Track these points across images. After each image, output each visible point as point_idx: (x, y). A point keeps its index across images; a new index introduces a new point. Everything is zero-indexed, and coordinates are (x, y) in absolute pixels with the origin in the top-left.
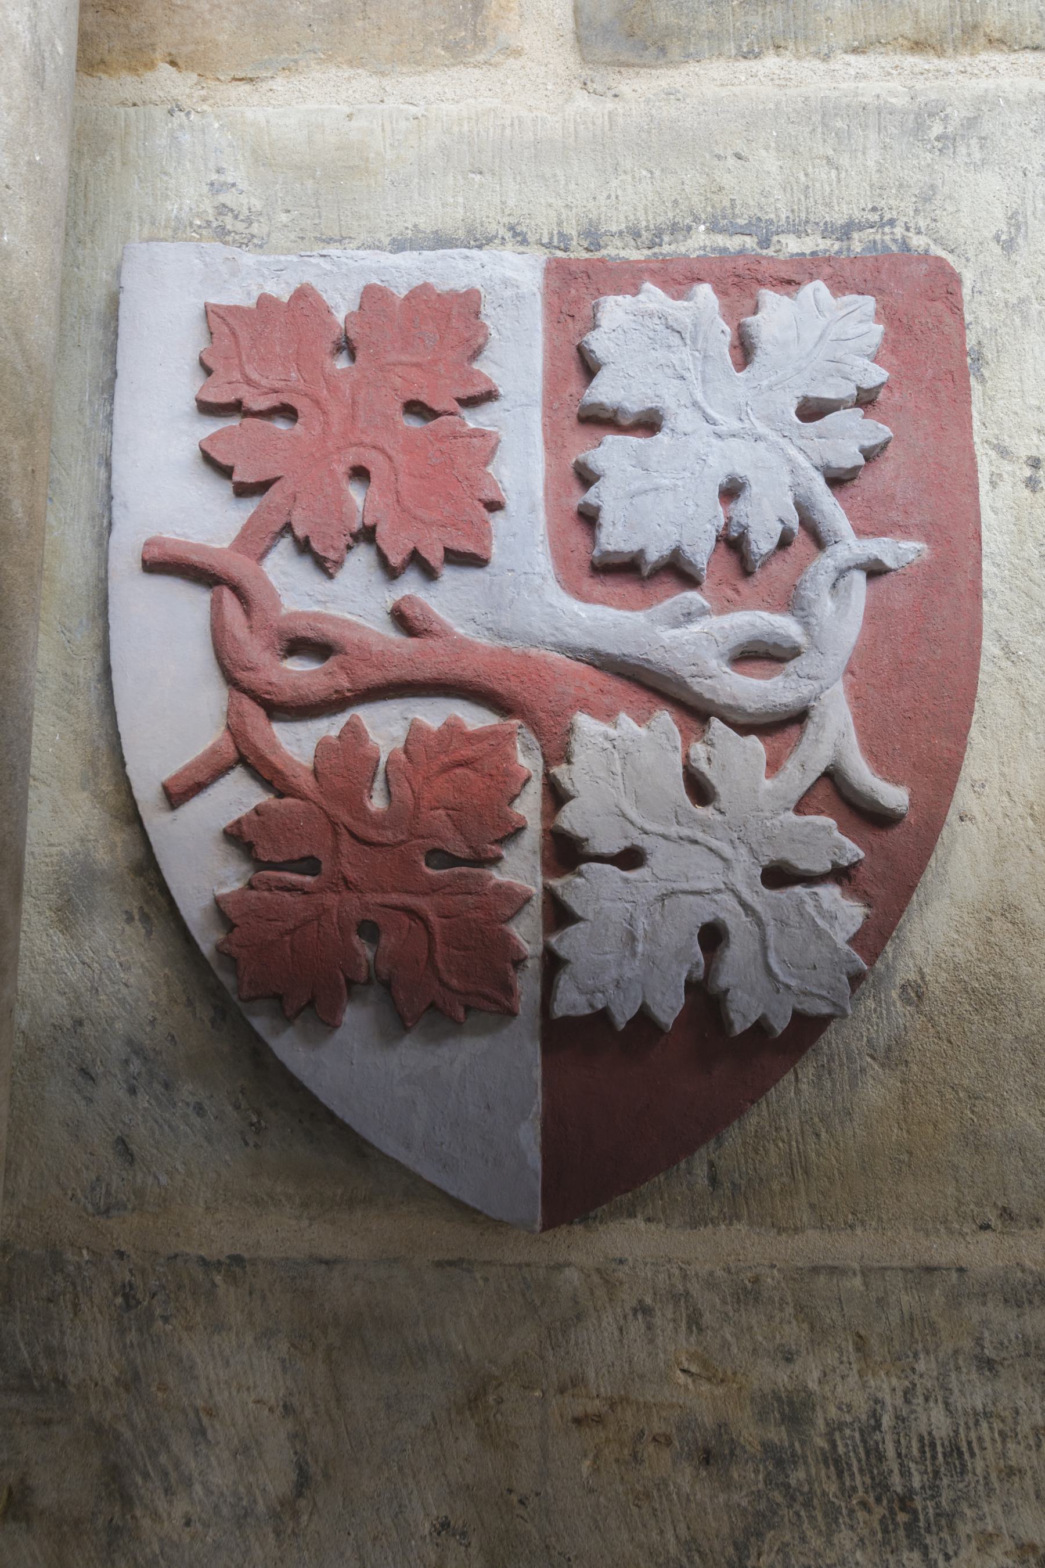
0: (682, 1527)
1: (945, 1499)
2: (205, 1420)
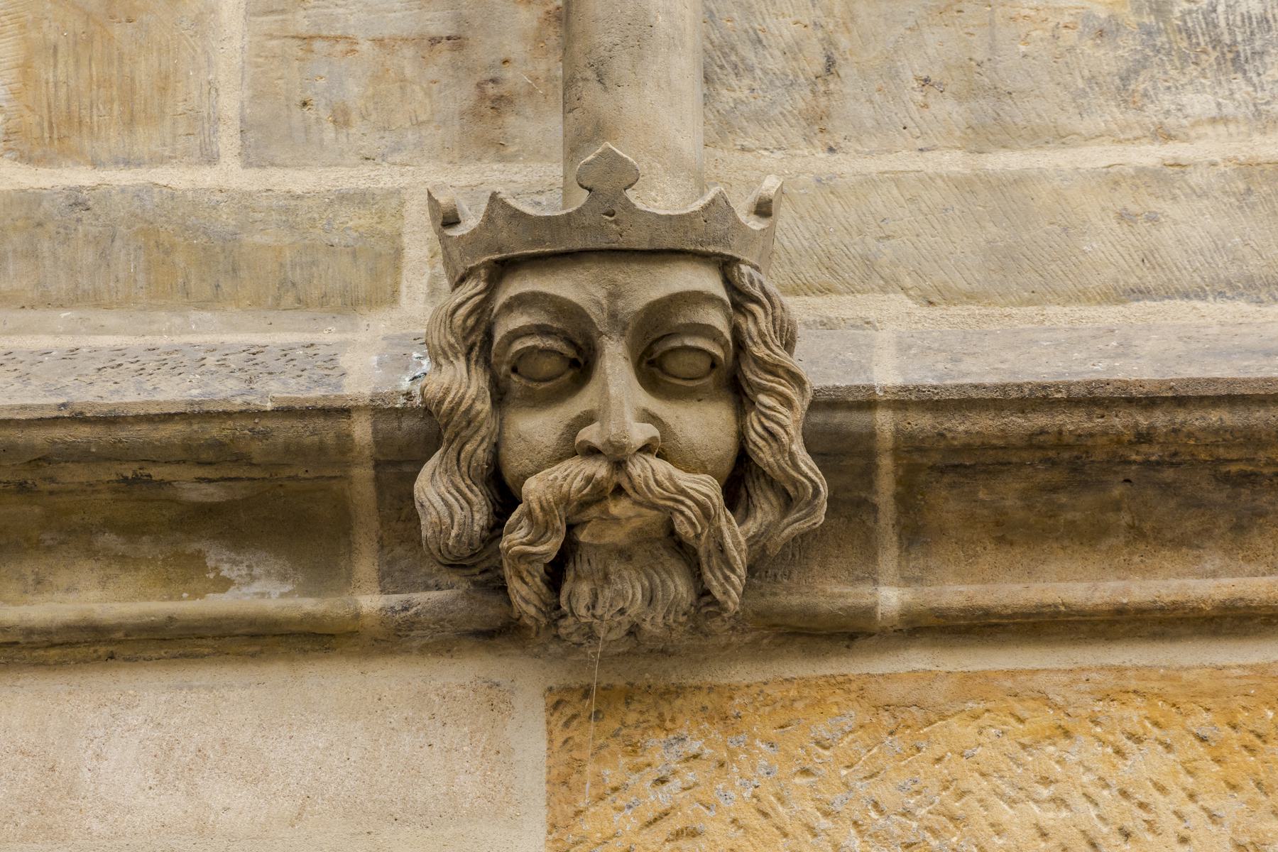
0: (1086, 73)
1: (1258, 44)
2: (761, 34)
